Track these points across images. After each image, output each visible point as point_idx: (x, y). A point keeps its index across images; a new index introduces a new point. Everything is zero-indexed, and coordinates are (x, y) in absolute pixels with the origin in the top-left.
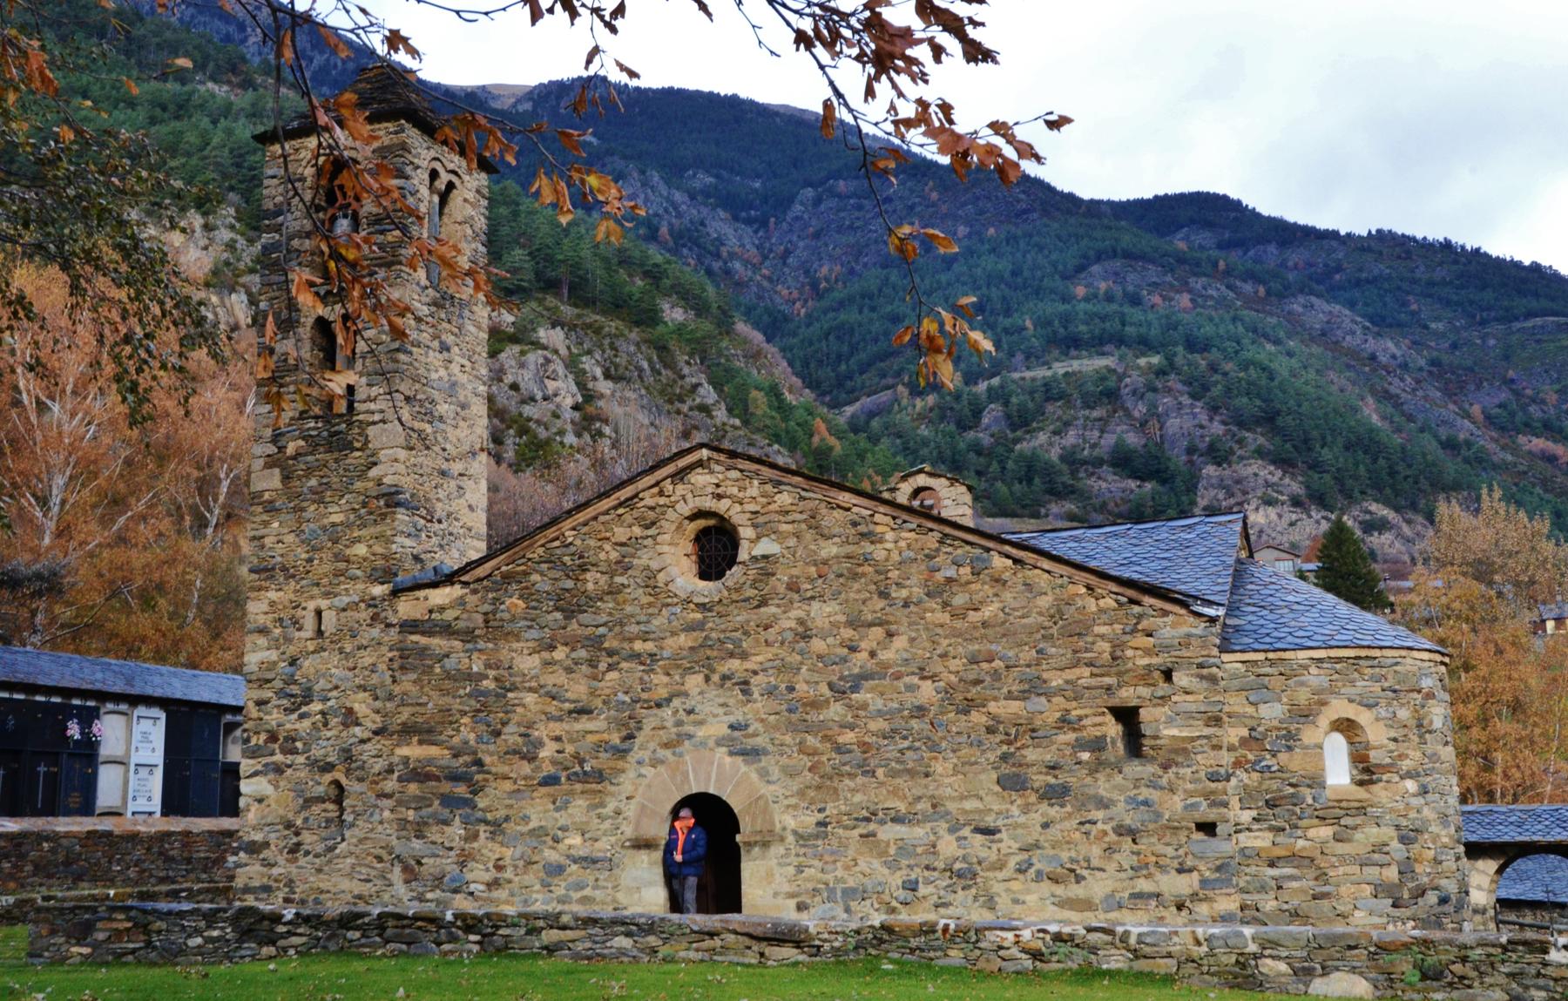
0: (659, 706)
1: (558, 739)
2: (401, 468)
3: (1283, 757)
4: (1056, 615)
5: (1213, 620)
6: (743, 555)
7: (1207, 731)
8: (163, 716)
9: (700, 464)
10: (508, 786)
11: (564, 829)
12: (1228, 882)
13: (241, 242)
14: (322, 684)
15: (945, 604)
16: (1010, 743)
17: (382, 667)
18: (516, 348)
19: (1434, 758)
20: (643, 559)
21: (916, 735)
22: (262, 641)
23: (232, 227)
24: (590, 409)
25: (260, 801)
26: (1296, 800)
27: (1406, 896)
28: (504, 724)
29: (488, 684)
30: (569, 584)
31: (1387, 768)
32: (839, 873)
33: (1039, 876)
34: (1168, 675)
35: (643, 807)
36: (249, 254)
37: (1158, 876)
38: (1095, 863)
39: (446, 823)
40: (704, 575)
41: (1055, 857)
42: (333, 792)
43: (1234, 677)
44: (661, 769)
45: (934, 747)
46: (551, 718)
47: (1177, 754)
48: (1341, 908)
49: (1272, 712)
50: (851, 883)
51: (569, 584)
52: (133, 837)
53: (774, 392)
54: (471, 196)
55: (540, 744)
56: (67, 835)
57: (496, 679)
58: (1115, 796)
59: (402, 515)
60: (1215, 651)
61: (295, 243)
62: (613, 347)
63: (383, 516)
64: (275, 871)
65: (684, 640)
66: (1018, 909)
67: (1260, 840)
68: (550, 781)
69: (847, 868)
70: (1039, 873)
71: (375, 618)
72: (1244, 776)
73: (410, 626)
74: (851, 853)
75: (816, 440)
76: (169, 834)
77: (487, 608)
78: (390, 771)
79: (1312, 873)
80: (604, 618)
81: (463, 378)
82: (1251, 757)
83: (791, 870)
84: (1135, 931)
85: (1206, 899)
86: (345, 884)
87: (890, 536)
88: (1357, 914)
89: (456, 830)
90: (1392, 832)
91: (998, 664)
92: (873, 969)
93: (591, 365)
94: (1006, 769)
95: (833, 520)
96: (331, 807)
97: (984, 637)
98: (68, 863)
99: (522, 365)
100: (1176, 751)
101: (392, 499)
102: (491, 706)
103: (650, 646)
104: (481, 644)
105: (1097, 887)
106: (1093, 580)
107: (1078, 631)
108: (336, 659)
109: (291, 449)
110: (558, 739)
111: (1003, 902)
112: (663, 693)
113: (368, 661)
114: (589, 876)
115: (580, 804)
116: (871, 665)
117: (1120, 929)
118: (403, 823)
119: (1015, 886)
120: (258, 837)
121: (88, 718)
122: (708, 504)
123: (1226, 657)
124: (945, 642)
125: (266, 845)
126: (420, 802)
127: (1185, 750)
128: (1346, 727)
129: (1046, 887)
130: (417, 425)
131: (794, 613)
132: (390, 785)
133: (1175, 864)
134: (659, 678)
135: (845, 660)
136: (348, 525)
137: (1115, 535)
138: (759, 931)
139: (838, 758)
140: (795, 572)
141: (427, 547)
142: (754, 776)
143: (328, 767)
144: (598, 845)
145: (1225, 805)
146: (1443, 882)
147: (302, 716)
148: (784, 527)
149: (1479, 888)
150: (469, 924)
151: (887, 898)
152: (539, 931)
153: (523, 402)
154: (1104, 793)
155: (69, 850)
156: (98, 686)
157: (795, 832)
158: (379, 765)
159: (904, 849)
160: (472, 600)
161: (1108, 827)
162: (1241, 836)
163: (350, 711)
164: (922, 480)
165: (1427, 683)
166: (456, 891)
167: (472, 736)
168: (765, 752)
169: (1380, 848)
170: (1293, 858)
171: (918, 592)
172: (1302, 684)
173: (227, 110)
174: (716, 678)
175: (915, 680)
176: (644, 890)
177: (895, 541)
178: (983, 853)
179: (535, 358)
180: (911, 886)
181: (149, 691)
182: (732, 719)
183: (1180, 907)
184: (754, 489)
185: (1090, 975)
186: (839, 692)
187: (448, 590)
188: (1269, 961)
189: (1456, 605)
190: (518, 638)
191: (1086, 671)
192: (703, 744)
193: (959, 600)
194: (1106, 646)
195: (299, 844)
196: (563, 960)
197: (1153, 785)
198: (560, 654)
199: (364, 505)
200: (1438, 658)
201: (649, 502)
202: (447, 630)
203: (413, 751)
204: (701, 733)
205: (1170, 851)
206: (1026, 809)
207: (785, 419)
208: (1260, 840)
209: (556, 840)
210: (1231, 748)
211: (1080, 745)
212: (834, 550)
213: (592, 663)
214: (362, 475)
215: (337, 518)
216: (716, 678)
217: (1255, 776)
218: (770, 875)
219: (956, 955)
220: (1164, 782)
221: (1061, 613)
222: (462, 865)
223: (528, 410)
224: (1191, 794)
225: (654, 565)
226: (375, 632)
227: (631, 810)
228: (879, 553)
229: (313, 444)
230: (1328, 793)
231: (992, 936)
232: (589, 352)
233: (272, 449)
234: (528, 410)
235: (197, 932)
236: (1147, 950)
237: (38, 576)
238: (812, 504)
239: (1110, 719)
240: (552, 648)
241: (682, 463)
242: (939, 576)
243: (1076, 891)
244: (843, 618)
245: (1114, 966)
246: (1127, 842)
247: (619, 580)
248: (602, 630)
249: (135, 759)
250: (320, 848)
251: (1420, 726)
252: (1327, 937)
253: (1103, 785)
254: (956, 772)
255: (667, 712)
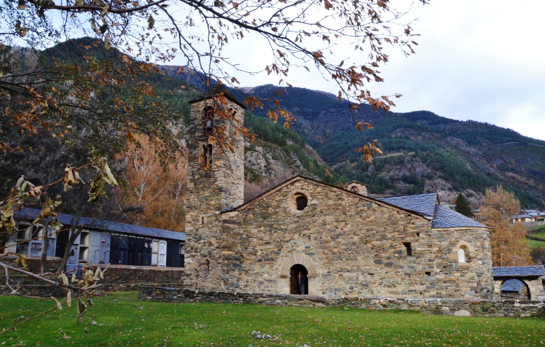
0: (287, 242)
1: (262, 250)
2: (223, 182)
3: (448, 255)
4: (389, 219)
5: (429, 220)
6: (309, 204)
7: (428, 249)
8: (166, 242)
9: (297, 181)
10: (249, 262)
11: (263, 273)
12: (433, 287)
13: (184, 127)
14: (204, 236)
15: (361, 216)
16: (377, 252)
17: (218, 231)
18: (250, 152)
19: (486, 255)
20: (283, 205)
21: (353, 250)
22: (189, 225)
23: (182, 124)
24: (269, 167)
25: (189, 264)
26: (451, 266)
27: (479, 290)
28: (248, 246)
29: (244, 236)
30: (265, 211)
31: (474, 258)
32: (333, 285)
33: (385, 286)
34: (418, 234)
35: (283, 268)
36: (186, 129)
37: (416, 286)
38: (399, 282)
39: (234, 270)
40: (298, 209)
41: (389, 281)
42: (206, 262)
43: (435, 235)
44: (288, 258)
45: (358, 253)
46: (260, 245)
47: (420, 255)
48: (462, 294)
49: (445, 244)
50: (336, 287)
51: (265, 211)
52: (160, 271)
53: (315, 162)
54: (240, 114)
55: (257, 251)
56: (146, 270)
57: (246, 235)
58: (404, 265)
59: (223, 194)
60: (430, 228)
61: (198, 127)
62: (274, 151)
63: (219, 194)
64: (193, 281)
65: (294, 225)
66: (379, 294)
67: (442, 276)
68: (260, 260)
69: (335, 283)
70: (385, 285)
71: (216, 219)
72: (438, 260)
73: (225, 221)
74: (336, 279)
75: (326, 174)
76: (168, 271)
77: (244, 217)
78: (220, 257)
79: (455, 285)
80: (273, 220)
81: (238, 159)
82: (439, 255)
83: (321, 284)
84: (410, 300)
85: (428, 291)
86: (210, 285)
87: (346, 199)
88: (466, 295)
89: (237, 272)
90: (476, 274)
91: (374, 231)
92: (342, 309)
93: (269, 156)
94: (376, 259)
95: (331, 195)
96: (206, 266)
97: (370, 225)
98: (146, 277)
99: (252, 156)
100: (420, 254)
101: (221, 190)
102: (245, 241)
103: (285, 227)
104: (243, 226)
105: (400, 288)
106: (399, 210)
107: (395, 223)
108: (207, 229)
109: (196, 178)
110: (262, 250)
111: (375, 292)
112: (288, 239)
113: (215, 230)
114: (270, 284)
115: (267, 267)
116: (341, 232)
117: (406, 299)
118: (224, 270)
119: (378, 288)
120: (189, 273)
121: (149, 242)
122: (300, 191)
123: (433, 230)
124: (360, 226)
125: (191, 275)
126: (228, 265)
127: (422, 254)
128: (464, 247)
129: (387, 288)
130: (227, 171)
131: (322, 218)
132: (220, 261)
133: (420, 283)
134: (287, 235)
135: (335, 231)
136: (210, 196)
137: (404, 198)
138: (313, 299)
139: (333, 256)
140: (322, 208)
141: (229, 202)
142: (311, 260)
143: (205, 256)
144: (272, 277)
145: (433, 267)
146: (488, 287)
147: (199, 243)
148: (319, 197)
149: (497, 288)
150: (240, 295)
151: (345, 291)
152: (258, 298)
153: (252, 165)
154: (401, 264)
155: (146, 274)
156: (152, 235)
157: (322, 274)
158: (217, 256)
159: (350, 279)
160: (240, 215)
161: (402, 273)
162: (437, 276)
163: (210, 242)
164: (354, 184)
165: (484, 236)
166: (237, 287)
167: (240, 249)
168: (314, 254)
169: (472, 278)
170: (450, 281)
171: (353, 213)
172: (453, 236)
173: (182, 96)
174: (302, 235)
175: (353, 236)
176: (284, 288)
177: (347, 200)
178: (370, 280)
179: (255, 154)
180: (352, 288)
181: (163, 236)
182: (306, 245)
183: (421, 294)
184: (311, 187)
185: (398, 311)
186: (333, 239)
187: (234, 212)
188: (444, 307)
189: (491, 216)
190: (252, 224)
191: (397, 233)
192: (298, 252)
193: (364, 215)
194: (402, 227)
195: (198, 275)
196: (264, 305)
197: (414, 262)
198: (262, 229)
199: (214, 191)
200: (487, 229)
201: (285, 190)
202: (234, 222)
203: (226, 252)
204: (298, 249)
205: (418, 279)
206: (381, 269)
207: (318, 169)
208: (442, 276)
209: (261, 275)
210: (434, 253)
211: (395, 252)
212: (332, 203)
213: (270, 231)
214: (213, 184)
215: (207, 194)
216: (302, 235)
217: (441, 260)
218: (315, 285)
219: (364, 306)
220: (417, 262)
221: (390, 218)
222: (238, 281)
223: (253, 167)
224: (424, 265)
225: (286, 206)
226: (217, 223)
227: (280, 268)
228: (343, 203)
229: (202, 176)
230: (459, 264)
231: (373, 301)
232: (268, 153)
233: (192, 177)
234: (253, 167)
235: (176, 295)
236: (413, 304)
237: (138, 208)
238: (326, 191)
239: (403, 245)
240: (260, 227)
241: (293, 180)
242: (359, 209)
243: (394, 289)
244: (334, 220)
245: (404, 308)
246: (407, 278)
247: (277, 210)
248: (273, 223)
249: (160, 253)
250: (204, 276)
251: (482, 247)
252: (459, 301)
253: (401, 263)
254: (363, 259)
255: (289, 244)
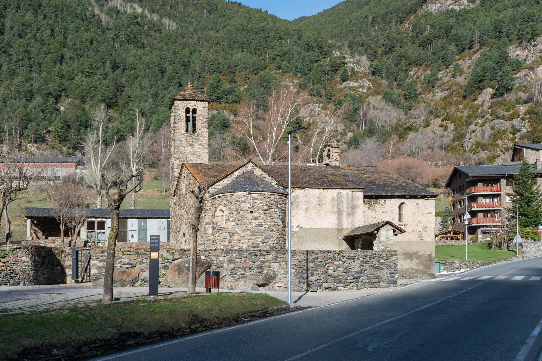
19: (243, 216)
90: (228, 234)
169: (225, 237)
